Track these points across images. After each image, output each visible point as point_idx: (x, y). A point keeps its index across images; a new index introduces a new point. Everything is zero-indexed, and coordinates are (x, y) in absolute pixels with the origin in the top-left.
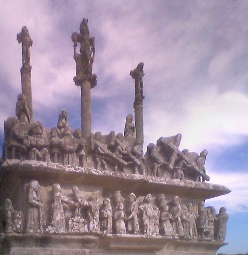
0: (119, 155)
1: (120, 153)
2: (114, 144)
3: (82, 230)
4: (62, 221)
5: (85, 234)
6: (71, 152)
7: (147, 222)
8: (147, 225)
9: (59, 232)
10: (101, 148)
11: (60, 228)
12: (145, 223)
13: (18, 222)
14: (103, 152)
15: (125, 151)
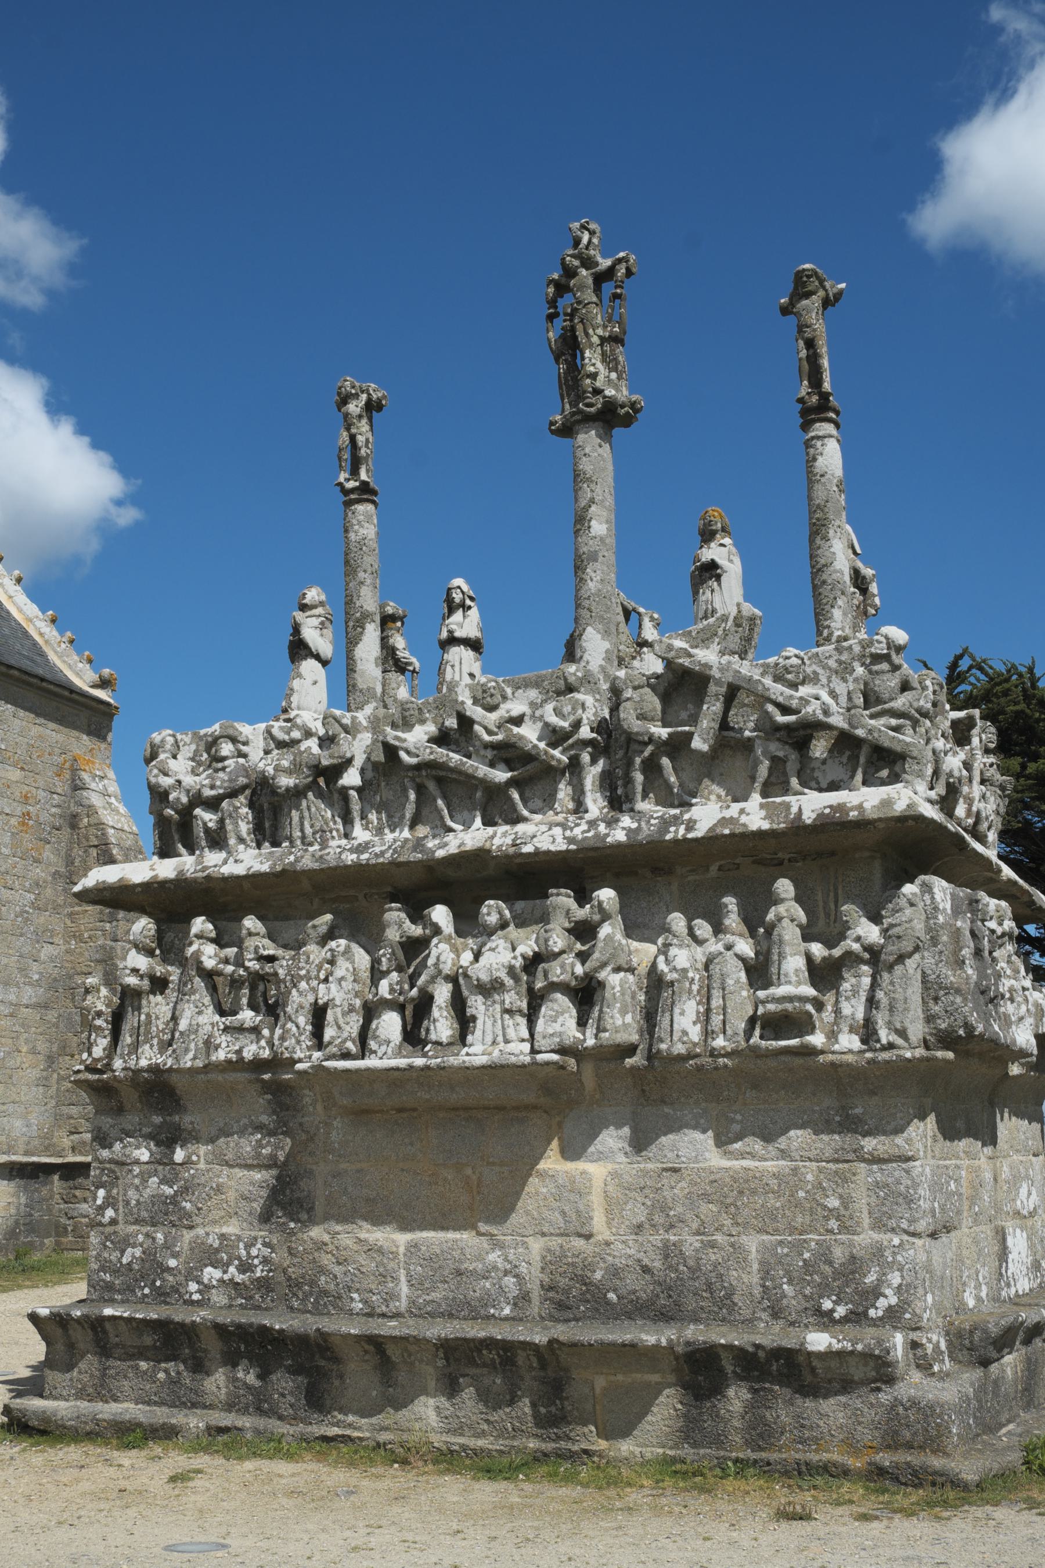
0: (482, 752)
1: (487, 746)
2: (456, 726)
3: (249, 1052)
4: (194, 1029)
5: (258, 1065)
6: (297, 794)
7: (476, 1005)
8: (474, 1019)
9: (182, 1066)
10: (408, 752)
11: (187, 1050)
12: (469, 1012)
13: (95, 1041)
14: (413, 761)
15: (497, 734)
